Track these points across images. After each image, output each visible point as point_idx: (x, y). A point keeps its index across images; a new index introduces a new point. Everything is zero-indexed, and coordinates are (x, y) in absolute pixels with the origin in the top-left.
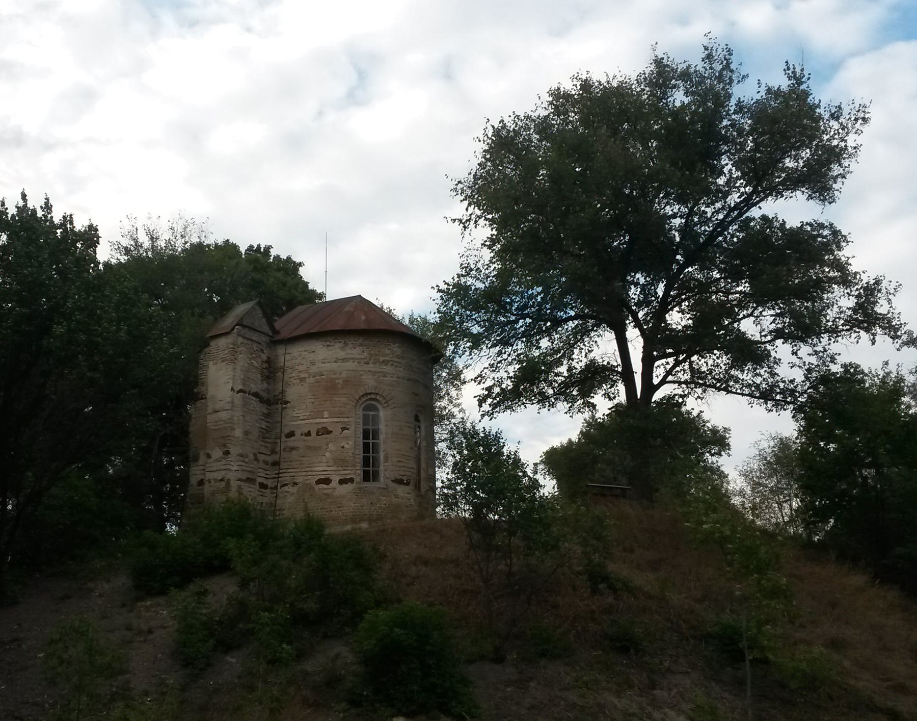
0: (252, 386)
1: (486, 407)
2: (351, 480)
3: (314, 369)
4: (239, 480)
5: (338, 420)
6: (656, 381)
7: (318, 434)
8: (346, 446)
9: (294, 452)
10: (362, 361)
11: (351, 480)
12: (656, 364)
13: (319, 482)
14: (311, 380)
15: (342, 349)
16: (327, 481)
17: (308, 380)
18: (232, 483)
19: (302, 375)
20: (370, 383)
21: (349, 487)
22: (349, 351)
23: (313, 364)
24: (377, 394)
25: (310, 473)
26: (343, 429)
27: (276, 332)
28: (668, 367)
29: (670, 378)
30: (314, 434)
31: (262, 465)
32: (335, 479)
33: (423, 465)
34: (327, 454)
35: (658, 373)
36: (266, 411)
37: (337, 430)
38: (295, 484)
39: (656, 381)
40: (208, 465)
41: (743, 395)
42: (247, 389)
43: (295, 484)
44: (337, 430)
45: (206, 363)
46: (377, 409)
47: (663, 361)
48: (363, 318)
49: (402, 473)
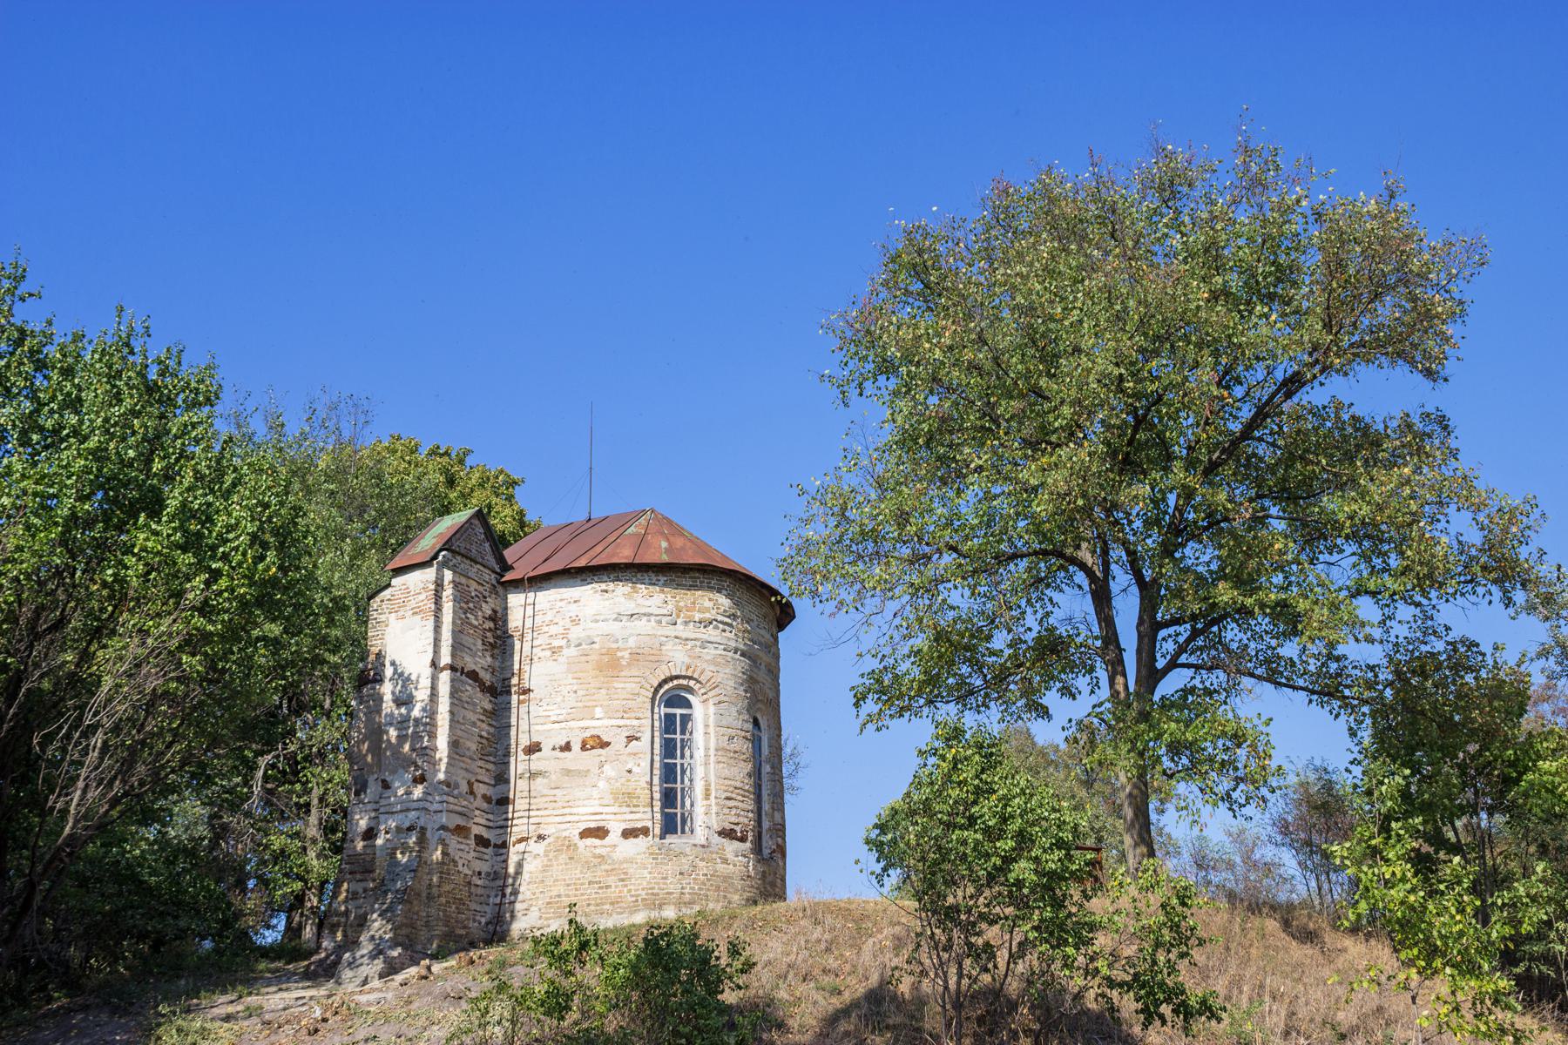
0: (468, 659)
1: (870, 706)
2: (645, 831)
3: (576, 633)
4: (443, 828)
5: (621, 722)
6: (1161, 663)
7: (584, 748)
8: (635, 769)
9: (539, 780)
10: (665, 620)
11: (645, 831)
12: (1163, 633)
13: (585, 834)
14: (572, 652)
15: (628, 596)
16: (600, 832)
17: (565, 651)
18: (429, 834)
19: (556, 643)
20: (678, 659)
21: (642, 842)
22: (640, 601)
23: (576, 621)
24: (691, 678)
25: (568, 818)
26: (631, 738)
27: (506, 567)
28: (1181, 639)
29: (1183, 659)
30: (576, 747)
31: (480, 803)
32: (616, 828)
33: (766, 807)
34: (601, 784)
35: (1166, 646)
36: (489, 707)
37: (618, 741)
38: (541, 837)
39: (1161, 663)
40: (383, 802)
41: (1294, 688)
42: (459, 664)
43: (541, 837)
44: (618, 741)
45: (383, 617)
46: (689, 706)
47: (1171, 630)
48: (664, 544)
49: (733, 819)
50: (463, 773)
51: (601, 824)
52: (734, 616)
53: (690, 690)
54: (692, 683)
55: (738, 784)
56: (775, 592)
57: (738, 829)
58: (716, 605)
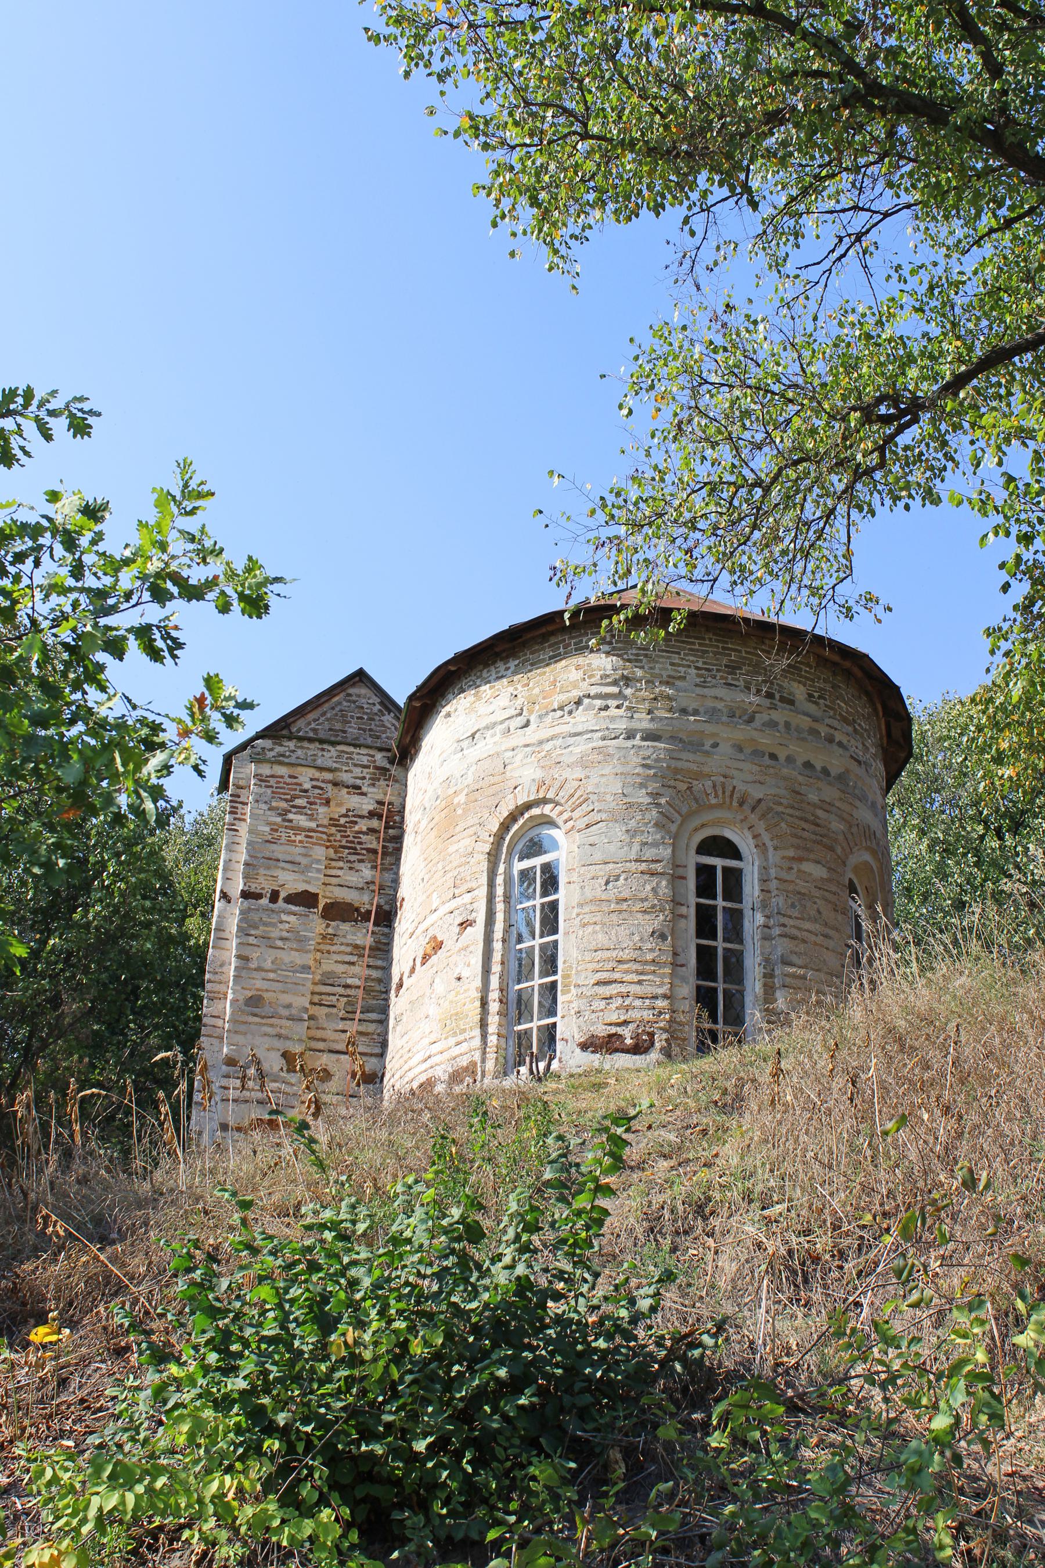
15: (471, 710)
20: (526, 778)
24: (545, 801)
49: (614, 1018)
50: (267, 1042)
51: (430, 1074)
52: (627, 680)
53: (552, 823)
54: (547, 809)
55: (625, 955)
56: (605, 611)
57: (627, 1032)
58: (588, 674)
